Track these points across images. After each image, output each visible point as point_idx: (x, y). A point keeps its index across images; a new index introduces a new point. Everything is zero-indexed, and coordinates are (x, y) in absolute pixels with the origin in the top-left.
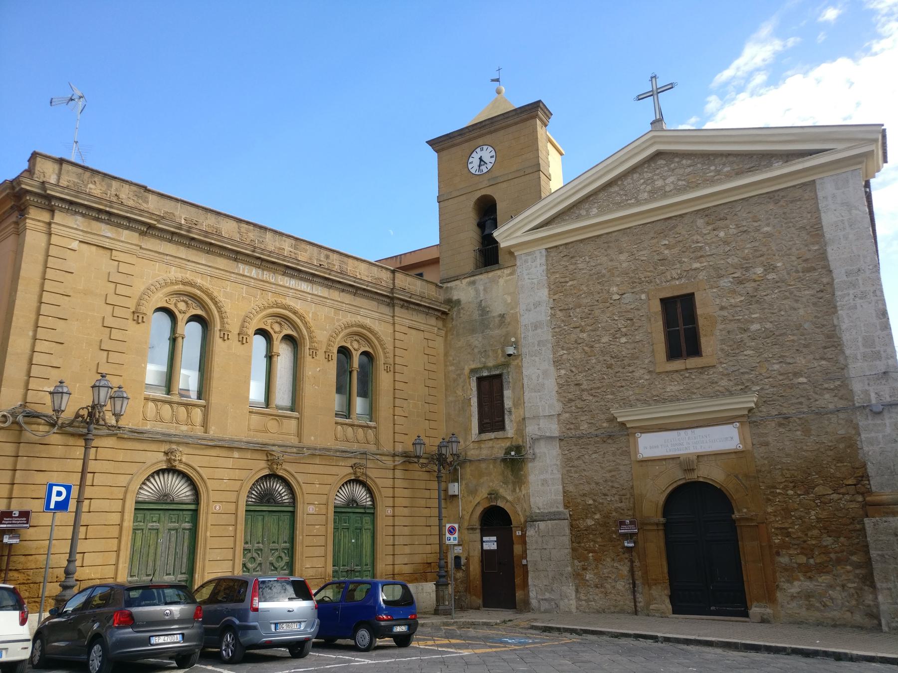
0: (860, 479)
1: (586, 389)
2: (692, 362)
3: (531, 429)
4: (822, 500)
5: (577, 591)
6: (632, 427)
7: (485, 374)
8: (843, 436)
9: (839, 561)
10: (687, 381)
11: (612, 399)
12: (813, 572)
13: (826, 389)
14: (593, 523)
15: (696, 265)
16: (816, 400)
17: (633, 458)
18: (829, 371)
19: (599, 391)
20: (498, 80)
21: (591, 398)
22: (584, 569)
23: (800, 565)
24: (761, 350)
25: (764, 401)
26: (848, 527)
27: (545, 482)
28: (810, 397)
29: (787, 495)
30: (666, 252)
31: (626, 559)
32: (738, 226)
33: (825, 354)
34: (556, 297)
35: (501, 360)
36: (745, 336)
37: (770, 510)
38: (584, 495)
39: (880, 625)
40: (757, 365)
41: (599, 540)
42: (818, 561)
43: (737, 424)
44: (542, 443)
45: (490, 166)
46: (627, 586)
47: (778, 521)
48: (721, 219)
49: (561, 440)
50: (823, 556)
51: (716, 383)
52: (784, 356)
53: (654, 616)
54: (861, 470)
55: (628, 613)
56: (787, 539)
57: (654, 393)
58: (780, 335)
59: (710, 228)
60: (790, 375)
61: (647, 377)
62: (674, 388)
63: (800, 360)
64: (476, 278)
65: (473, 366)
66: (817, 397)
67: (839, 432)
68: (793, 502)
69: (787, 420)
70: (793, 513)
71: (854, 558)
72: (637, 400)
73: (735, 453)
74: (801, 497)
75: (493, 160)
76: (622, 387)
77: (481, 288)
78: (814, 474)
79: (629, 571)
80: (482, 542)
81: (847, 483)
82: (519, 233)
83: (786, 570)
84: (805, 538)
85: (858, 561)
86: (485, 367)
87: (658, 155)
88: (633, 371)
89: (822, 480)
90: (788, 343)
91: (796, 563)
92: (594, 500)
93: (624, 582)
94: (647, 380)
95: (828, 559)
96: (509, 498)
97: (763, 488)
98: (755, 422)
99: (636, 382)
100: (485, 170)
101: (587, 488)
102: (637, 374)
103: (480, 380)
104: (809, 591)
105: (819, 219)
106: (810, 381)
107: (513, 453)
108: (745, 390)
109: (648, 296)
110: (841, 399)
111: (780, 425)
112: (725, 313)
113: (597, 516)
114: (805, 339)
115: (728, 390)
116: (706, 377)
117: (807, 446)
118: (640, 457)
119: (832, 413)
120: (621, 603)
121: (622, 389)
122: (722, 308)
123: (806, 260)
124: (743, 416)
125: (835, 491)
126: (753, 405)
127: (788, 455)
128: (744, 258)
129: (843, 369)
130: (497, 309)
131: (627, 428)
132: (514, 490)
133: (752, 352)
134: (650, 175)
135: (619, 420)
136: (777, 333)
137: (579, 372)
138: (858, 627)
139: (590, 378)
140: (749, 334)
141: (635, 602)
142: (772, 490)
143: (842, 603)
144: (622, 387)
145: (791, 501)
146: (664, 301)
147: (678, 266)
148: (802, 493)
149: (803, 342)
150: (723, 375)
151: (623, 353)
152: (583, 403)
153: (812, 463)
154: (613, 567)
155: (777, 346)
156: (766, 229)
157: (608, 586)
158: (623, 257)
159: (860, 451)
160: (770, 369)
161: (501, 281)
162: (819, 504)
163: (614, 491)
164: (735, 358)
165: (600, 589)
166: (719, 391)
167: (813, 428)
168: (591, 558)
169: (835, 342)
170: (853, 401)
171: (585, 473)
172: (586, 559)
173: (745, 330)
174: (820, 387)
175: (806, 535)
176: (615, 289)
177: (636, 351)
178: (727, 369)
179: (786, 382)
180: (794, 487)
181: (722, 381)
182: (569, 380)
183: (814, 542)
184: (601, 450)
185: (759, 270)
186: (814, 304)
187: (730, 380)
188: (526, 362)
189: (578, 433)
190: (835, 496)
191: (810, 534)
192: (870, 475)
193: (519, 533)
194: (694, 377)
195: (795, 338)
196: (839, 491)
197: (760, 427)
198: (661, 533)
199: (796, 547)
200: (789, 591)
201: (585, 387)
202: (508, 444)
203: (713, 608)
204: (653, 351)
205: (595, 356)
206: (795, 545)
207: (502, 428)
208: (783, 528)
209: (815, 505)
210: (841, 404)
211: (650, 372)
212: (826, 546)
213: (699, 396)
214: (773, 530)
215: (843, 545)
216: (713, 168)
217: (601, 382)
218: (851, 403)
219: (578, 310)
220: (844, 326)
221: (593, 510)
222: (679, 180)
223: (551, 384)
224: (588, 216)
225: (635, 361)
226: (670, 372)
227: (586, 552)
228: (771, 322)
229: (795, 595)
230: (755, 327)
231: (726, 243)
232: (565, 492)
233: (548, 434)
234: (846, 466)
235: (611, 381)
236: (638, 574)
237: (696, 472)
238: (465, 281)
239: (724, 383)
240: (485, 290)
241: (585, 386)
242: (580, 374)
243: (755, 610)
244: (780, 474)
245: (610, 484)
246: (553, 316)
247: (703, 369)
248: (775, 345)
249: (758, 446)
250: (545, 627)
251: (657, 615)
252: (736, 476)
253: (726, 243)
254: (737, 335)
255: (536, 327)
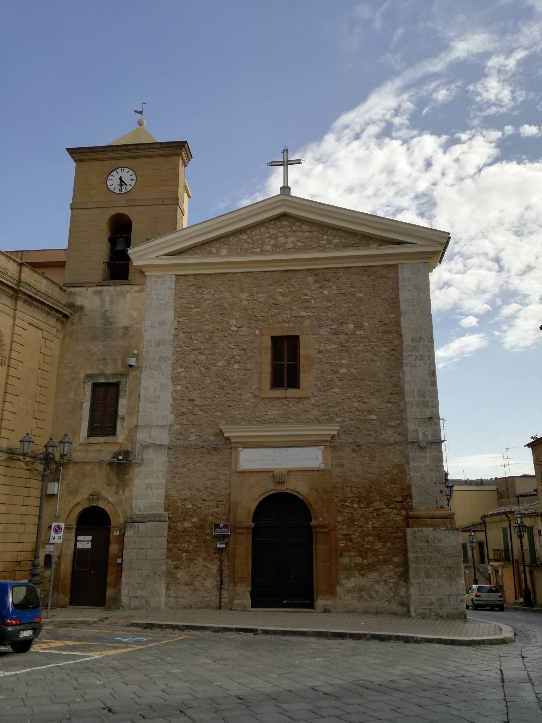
0: (405, 497)
1: (198, 405)
2: (292, 392)
3: (142, 436)
4: (378, 512)
5: (168, 588)
6: (235, 442)
7: (102, 380)
8: (397, 463)
9: (385, 562)
10: (285, 407)
11: (220, 416)
12: (366, 570)
13: (389, 426)
14: (190, 525)
15: (303, 314)
16: (382, 434)
17: (233, 469)
18: (393, 412)
19: (209, 408)
20: (140, 113)
21: (202, 413)
22: (177, 568)
23: (356, 564)
24: (345, 390)
25: (345, 430)
26: (394, 535)
27: (149, 486)
28: (378, 431)
29: (353, 507)
30: (280, 298)
31: (217, 558)
32: (338, 288)
33: (391, 398)
34: (180, 320)
35: (120, 369)
36: (334, 377)
37: (339, 519)
38: (185, 499)
39: (409, 611)
40: (341, 401)
41: (194, 541)
42: (370, 562)
43: (322, 447)
44: (151, 451)
45: (129, 188)
46: (215, 584)
47: (344, 529)
48: (326, 280)
49: (169, 448)
50: (373, 557)
51: (309, 412)
52: (362, 397)
53: (236, 610)
54: (406, 490)
55: (213, 608)
56: (349, 544)
57: (257, 415)
58: (361, 380)
59: (317, 285)
60: (365, 412)
61: (252, 400)
62: (275, 413)
63: (373, 401)
64: (104, 288)
65: (89, 372)
66: (382, 431)
67: (395, 460)
68: (357, 513)
69: (359, 448)
70: (356, 523)
71: (395, 559)
72: (242, 419)
73: (318, 471)
74: (363, 510)
75: (133, 183)
76: (230, 406)
77: (108, 299)
78: (374, 492)
79: (218, 570)
80: (76, 541)
81: (397, 500)
82: (153, 256)
83: (346, 568)
84: (363, 543)
85: (398, 561)
86: (102, 374)
87: (284, 216)
88: (241, 394)
89: (380, 497)
90: (366, 387)
91: (354, 563)
92: (193, 505)
93: (212, 580)
94: (252, 403)
95: (377, 560)
96: (111, 500)
97: (336, 501)
98: (335, 447)
99: (243, 404)
100: (124, 191)
101: (188, 493)
102: (244, 397)
103: (95, 386)
104: (361, 586)
105: (397, 294)
106: (378, 418)
107: (121, 458)
108: (330, 420)
109: (261, 332)
110: (399, 435)
111: (354, 451)
112: (321, 356)
113: (195, 519)
114: (379, 386)
115: (317, 419)
116: (301, 406)
117: (371, 469)
118: (240, 468)
119: (391, 445)
120: (208, 599)
121: (230, 408)
122: (320, 352)
123: (385, 325)
124: (327, 441)
125: (388, 506)
126: (335, 433)
127: (357, 476)
128: (340, 315)
129: (402, 412)
130: (122, 321)
131: (231, 443)
132: (117, 492)
133: (339, 390)
134: (275, 231)
135: (226, 435)
136: (358, 378)
137: (194, 390)
138: (393, 614)
139: (202, 396)
140: (338, 376)
141: (220, 598)
142: (343, 503)
143: (384, 595)
144: (230, 406)
145: (355, 513)
146: (274, 339)
147: (288, 311)
148: (364, 507)
149: (377, 388)
150: (314, 406)
151: (235, 377)
152: (194, 417)
153: (374, 483)
154: (203, 566)
155: (358, 388)
156: (359, 295)
157: (197, 584)
158: (244, 296)
159: (408, 476)
160: (351, 405)
161: (129, 296)
162: (375, 516)
163: (212, 497)
164: (325, 393)
165: (190, 587)
166: (310, 419)
167: (377, 455)
168: (184, 558)
169: (399, 390)
170: (407, 437)
171: (188, 480)
172: (180, 558)
173: (335, 372)
174: (385, 424)
175: (364, 540)
176: (234, 322)
177: (246, 377)
178: (318, 401)
179: (362, 417)
180: (359, 501)
181: (313, 411)
182: (184, 395)
183: (368, 546)
184: (205, 460)
185: (351, 326)
186: (388, 359)
187: (319, 411)
188: (145, 374)
189: (186, 443)
190: (387, 510)
191: (366, 539)
192: (413, 495)
193: (117, 533)
194: (291, 405)
195: (371, 383)
196: (390, 507)
197: (338, 451)
198: (250, 536)
199: (355, 550)
200: (346, 586)
201: (198, 403)
202: (117, 449)
203: (285, 602)
204: (260, 379)
205: (210, 377)
206: (355, 548)
207: (113, 432)
208: (348, 535)
209: (372, 516)
210: (399, 439)
211: (255, 396)
212: (376, 550)
213: (294, 421)
214: (340, 536)
215: (389, 549)
216: (325, 237)
217: (212, 401)
218: (405, 439)
219: (199, 334)
220: (406, 379)
221: (191, 513)
222: (298, 241)
223: (167, 398)
224: (218, 255)
225: (244, 386)
226: (273, 398)
227: (180, 552)
228: (355, 369)
229: (350, 589)
230: (343, 370)
231: (328, 300)
232: (167, 497)
233: (158, 442)
234: (397, 487)
235: (222, 400)
236: (226, 572)
237: (285, 484)
238: (91, 290)
239: (314, 412)
240: (112, 301)
241: (197, 402)
242: (194, 391)
243: (320, 602)
244: (350, 490)
245: (210, 490)
246: (176, 336)
247: (300, 399)
248: (356, 387)
249: (336, 467)
250: (146, 624)
251: (239, 609)
252: (317, 490)
253: (328, 300)
254: (329, 375)
255: (159, 344)
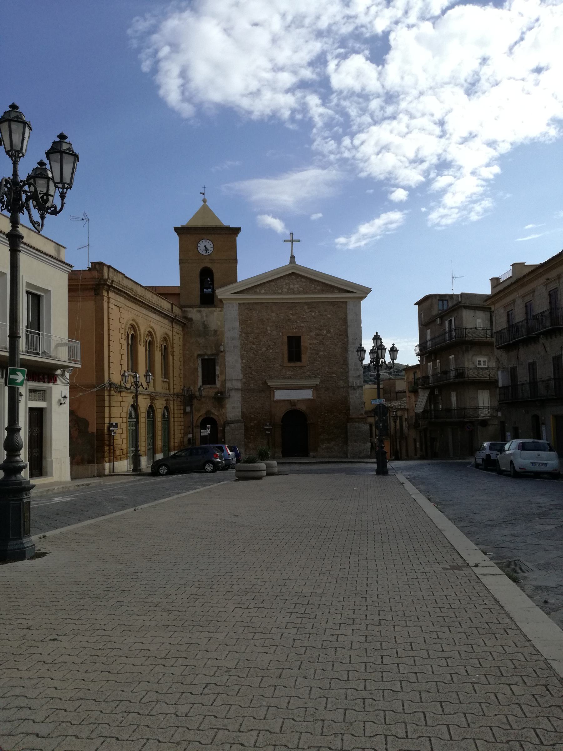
2: (298, 364)
3: (228, 385)
5: (245, 451)
7: (206, 357)
15: (302, 325)
20: (203, 194)
21: (256, 374)
25: (322, 382)
27: (233, 408)
30: (291, 316)
32: (319, 312)
34: (243, 326)
35: (214, 351)
37: (319, 420)
44: (233, 391)
45: (210, 252)
48: (313, 308)
49: (242, 390)
59: (309, 310)
62: (290, 373)
64: (202, 309)
65: (199, 353)
75: (212, 249)
77: (204, 315)
80: (201, 432)
82: (228, 293)
86: (206, 354)
87: (293, 274)
92: (254, 416)
96: (216, 414)
100: (208, 254)
103: (203, 360)
105: (347, 316)
107: (219, 395)
108: (315, 377)
109: (283, 333)
112: (311, 346)
113: (255, 422)
118: (275, 399)
119: (342, 388)
122: (310, 344)
123: (340, 331)
124: (314, 386)
125: (340, 414)
128: (320, 326)
130: (213, 327)
132: (219, 411)
134: (288, 281)
135: (268, 384)
146: (289, 338)
147: (295, 323)
156: (329, 316)
158: (273, 315)
161: (215, 313)
176: (269, 328)
185: (325, 332)
186: (341, 348)
188: (227, 354)
193: (221, 428)
202: (217, 390)
207: (214, 383)
211: (280, 366)
216: (313, 286)
219: (252, 334)
220: (350, 358)
222: (300, 287)
223: (239, 366)
224: (260, 294)
230: (321, 353)
231: (314, 318)
232: (242, 412)
233: (236, 388)
238: (195, 309)
239: (308, 373)
240: (206, 316)
241: (253, 368)
243: (312, 454)
246: (240, 335)
247: (301, 367)
253: (314, 318)
255: (233, 339)
